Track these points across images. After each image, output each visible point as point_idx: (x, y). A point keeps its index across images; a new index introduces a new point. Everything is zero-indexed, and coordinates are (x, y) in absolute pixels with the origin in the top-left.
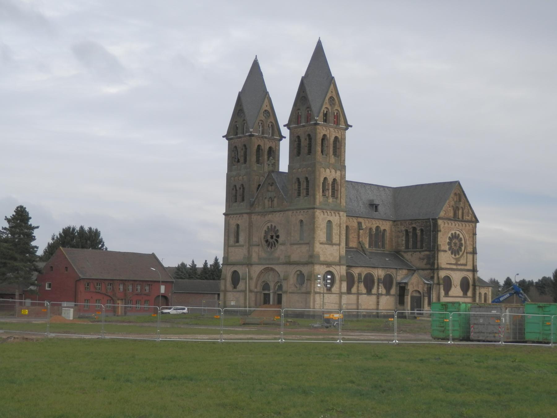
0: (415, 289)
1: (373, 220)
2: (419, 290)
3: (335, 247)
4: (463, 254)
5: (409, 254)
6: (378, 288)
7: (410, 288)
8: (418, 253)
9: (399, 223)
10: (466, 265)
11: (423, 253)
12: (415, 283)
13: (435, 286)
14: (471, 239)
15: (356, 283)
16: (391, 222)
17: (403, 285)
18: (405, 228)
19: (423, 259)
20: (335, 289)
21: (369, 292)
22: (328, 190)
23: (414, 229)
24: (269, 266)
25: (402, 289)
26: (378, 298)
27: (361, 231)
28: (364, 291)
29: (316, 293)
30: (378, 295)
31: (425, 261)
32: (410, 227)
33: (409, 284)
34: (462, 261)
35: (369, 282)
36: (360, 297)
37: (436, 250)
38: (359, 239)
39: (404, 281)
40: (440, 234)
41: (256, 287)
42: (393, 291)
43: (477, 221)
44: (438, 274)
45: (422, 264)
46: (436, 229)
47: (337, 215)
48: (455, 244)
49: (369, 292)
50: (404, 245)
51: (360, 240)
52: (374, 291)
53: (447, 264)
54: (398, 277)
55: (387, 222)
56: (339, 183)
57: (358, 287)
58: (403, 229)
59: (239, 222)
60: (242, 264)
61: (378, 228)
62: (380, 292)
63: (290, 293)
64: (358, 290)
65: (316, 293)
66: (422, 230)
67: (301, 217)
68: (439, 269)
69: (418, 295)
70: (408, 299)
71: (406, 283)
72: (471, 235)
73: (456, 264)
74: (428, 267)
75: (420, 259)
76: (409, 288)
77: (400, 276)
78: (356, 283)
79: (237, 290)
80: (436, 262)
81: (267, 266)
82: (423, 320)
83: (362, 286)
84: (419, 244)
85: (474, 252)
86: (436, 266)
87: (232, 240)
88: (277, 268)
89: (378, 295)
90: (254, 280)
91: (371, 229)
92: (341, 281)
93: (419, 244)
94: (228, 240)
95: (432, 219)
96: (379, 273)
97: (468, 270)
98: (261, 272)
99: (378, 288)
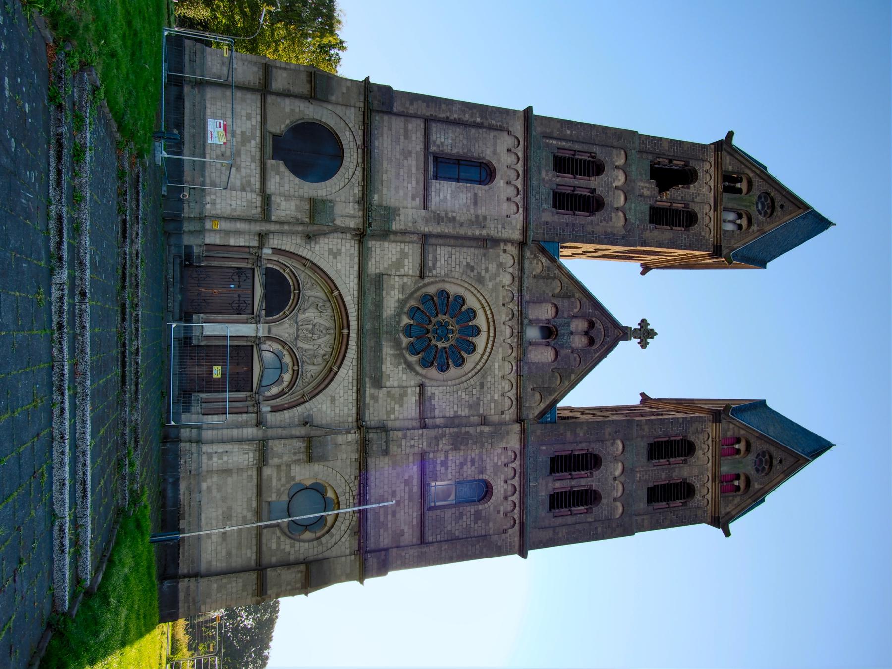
24: (353, 335)
41: (276, 251)
59: (499, 182)
60: (364, 201)
67: (500, 488)
79: (271, 162)
81: (354, 323)
87: (447, 141)
88: (347, 372)
90: (305, 252)
94: (447, 122)
98: (331, 286)
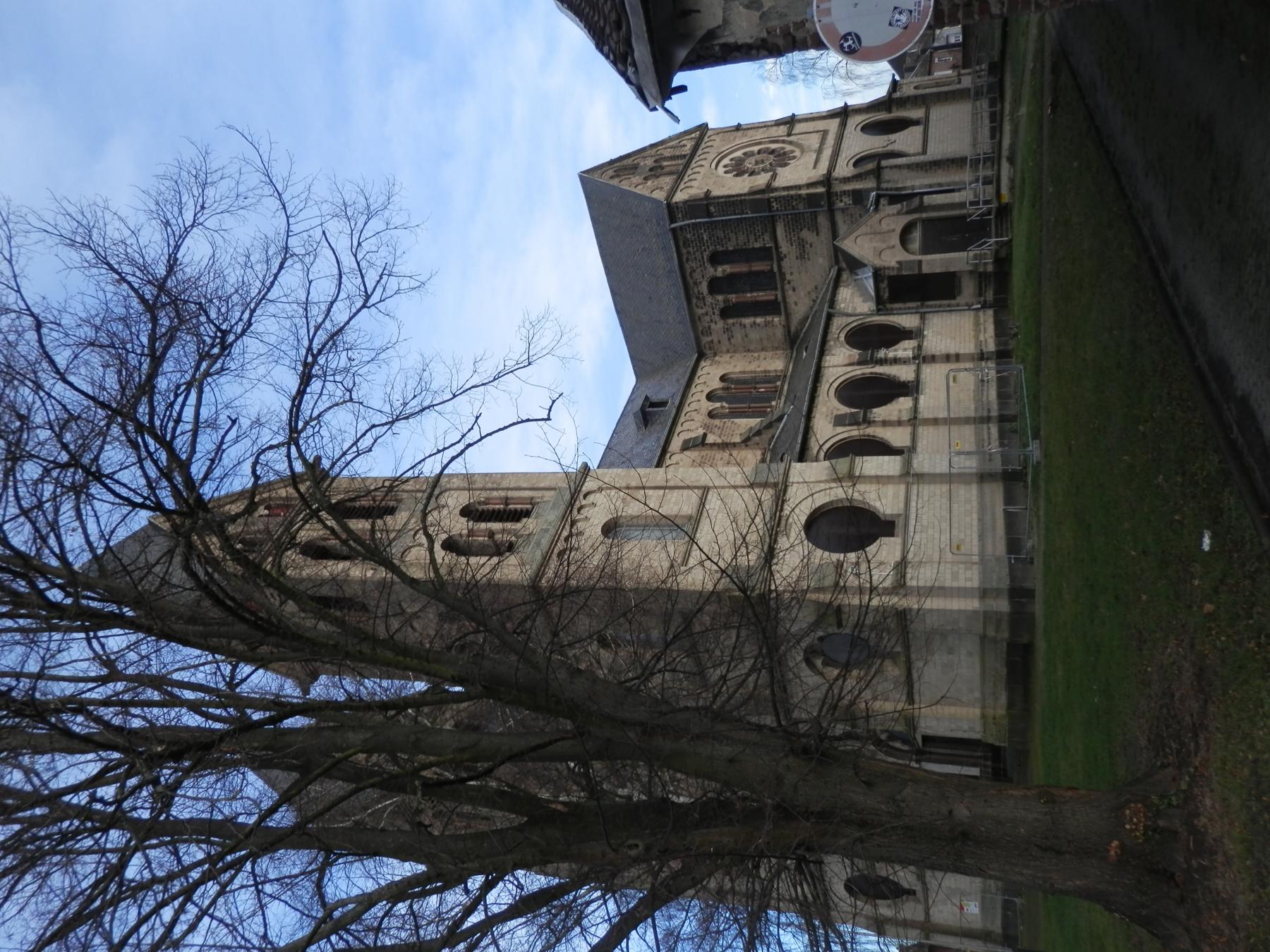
0: (896, 240)
1: (686, 409)
2: (899, 230)
3: (713, 502)
4: (791, 143)
5: (792, 297)
6: (896, 361)
7: (894, 258)
8: (786, 264)
9: (705, 340)
10: (825, 133)
11: (784, 247)
12: (877, 243)
13: (884, 185)
14: (750, 132)
15: (870, 431)
16: (703, 364)
17: (884, 285)
18: (717, 318)
19: (802, 244)
20: (885, 501)
21: (910, 389)
22: (491, 534)
23: (715, 286)
25: (902, 288)
26: (933, 359)
27: (711, 439)
28: (904, 403)
29: (900, 586)
30: (921, 358)
31: (806, 234)
32: (709, 300)
33: (878, 263)
34: (814, 141)
35: (866, 394)
36: (925, 413)
37: (766, 196)
38: (734, 445)
39: (870, 284)
40: (716, 192)
42: (907, 321)
43: (703, 128)
44: (846, 180)
45: (819, 244)
46: (704, 205)
47: (591, 498)
48: (757, 163)
49: (910, 389)
50: (769, 318)
51: (737, 439)
52: (904, 373)
53: (815, 167)
54: (859, 310)
55: (699, 373)
56: (484, 494)
57: (885, 423)
58: (721, 324)
61: (710, 397)
62: (910, 354)
63: (911, 699)
64: (899, 423)
65: (900, 586)
66: (715, 259)
68: (827, 180)
69: (917, 235)
70: (935, 263)
71: (878, 274)
72: (740, 133)
73: (819, 151)
74: (823, 221)
75: (802, 256)
76: (893, 264)
77: (855, 302)
78: (870, 431)
80: (804, 192)
82: (1012, 180)
83: (879, 413)
84: (758, 266)
85: (791, 121)
86: (821, 190)
89: (921, 358)
91: (711, 415)
92: (852, 478)
93: (758, 266)
95: (673, 220)
96: (841, 363)
97: (843, 125)
99: (896, 361)
